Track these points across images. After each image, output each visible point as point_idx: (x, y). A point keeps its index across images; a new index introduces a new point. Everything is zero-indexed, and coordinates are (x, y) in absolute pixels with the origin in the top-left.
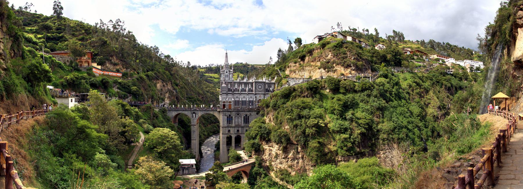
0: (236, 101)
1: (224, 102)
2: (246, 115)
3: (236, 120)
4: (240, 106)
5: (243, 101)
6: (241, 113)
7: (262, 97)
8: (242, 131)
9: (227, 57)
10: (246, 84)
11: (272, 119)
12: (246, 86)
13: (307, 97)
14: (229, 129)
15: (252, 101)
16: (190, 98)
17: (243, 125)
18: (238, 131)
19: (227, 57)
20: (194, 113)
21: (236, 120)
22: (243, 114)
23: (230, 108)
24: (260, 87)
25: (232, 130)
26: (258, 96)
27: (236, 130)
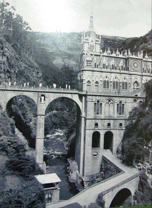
0: (105, 82)
1: (89, 82)
2: (121, 102)
4: (111, 88)
8: (114, 126)
14: (97, 121)
15: (126, 83)
17: (116, 115)
18: (109, 125)
20: (42, 95)
21: (107, 109)
22: (117, 100)
24: (136, 65)
25: (99, 122)
26: (133, 77)
27: (106, 124)
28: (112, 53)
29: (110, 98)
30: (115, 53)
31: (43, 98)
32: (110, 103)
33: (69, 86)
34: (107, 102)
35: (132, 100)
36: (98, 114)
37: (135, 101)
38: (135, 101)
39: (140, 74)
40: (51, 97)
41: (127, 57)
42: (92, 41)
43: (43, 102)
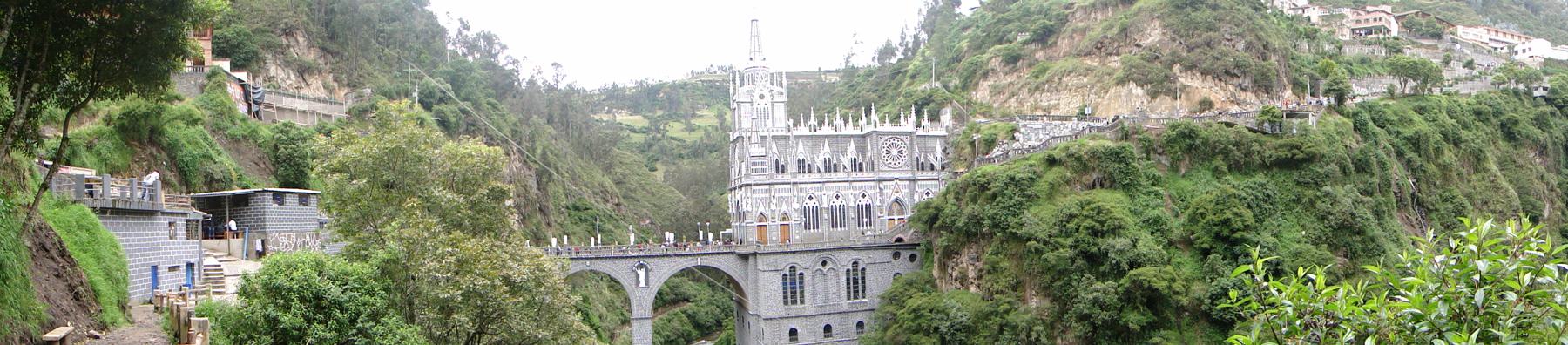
0: (806, 211)
1: (762, 217)
3: (820, 286)
4: (825, 228)
5: (833, 210)
6: (837, 254)
7: (904, 193)
9: (755, 36)
10: (838, 141)
11: (971, 275)
12: (814, 150)
13: (1102, 186)
15: (869, 208)
16: (577, 208)
17: (845, 304)
19: (755, 36)
20: (641, 266)
22: (845, 259)
23: (785, 238)
24: (894, 152)
28: (821, 123)
29: (824, 254)
30: (830, 123)
31: (642, 273)
32: (825, 269)
33: (711, 236)
34: (819, 266)
35: (887, 255)
36: (794, 302)
37: (896, 255)
38: (896, 255)
39: (909, 175)
40: (664, 271)
41: (866, 131)
42: (762, 97)
43: (643, 284)
